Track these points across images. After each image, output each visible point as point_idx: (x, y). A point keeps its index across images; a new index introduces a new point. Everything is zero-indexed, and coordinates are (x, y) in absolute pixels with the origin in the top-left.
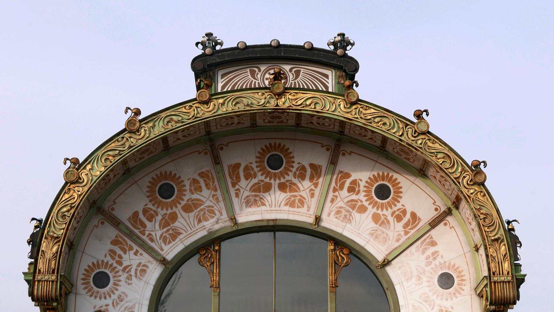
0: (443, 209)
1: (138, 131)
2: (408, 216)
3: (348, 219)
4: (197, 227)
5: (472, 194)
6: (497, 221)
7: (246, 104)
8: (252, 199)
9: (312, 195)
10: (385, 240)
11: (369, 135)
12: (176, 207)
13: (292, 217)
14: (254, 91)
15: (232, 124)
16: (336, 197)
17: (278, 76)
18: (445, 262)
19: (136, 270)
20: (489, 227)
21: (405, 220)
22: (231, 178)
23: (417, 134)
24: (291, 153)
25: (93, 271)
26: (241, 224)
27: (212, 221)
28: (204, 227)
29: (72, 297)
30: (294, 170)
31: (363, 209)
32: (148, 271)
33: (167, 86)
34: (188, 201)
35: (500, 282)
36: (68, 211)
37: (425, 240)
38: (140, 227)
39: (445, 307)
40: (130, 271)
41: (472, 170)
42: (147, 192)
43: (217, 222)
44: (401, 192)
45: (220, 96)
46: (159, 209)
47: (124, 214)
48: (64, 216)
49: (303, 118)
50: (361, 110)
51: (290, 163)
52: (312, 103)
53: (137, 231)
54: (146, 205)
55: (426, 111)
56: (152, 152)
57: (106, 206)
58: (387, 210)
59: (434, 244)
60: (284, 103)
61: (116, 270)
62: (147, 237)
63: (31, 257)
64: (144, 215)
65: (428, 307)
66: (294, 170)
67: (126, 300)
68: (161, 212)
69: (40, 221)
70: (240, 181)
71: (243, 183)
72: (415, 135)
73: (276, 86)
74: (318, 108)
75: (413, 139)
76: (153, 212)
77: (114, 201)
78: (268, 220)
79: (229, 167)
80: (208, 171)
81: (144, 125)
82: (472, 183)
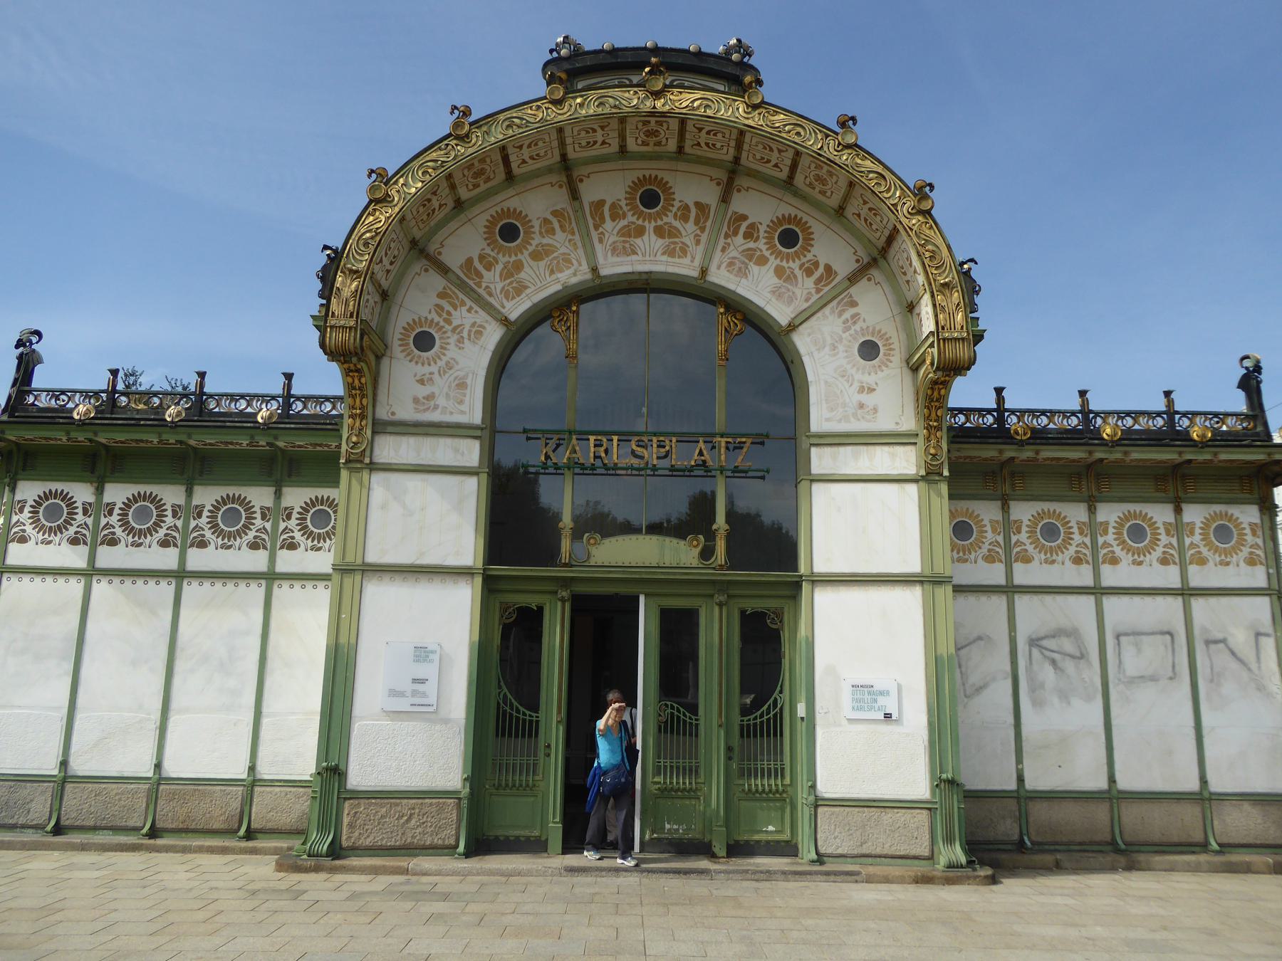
1: (467, 136)
2: (821, 269)
3: (743, 273)
4: (549, 279)
6: (948, 260)
8: (620, 246)
9: (698, 242)
10: (791, 300)
13: (671, 270)
19: (470, 331)
20: (937, 268)
21: (817, 274)
27: (568, 272)
29: (385, 362)
31: (762, 261)
32: (486, 333)
33: (511, 80)
36: (372, 238)
40: (462, 331)
41: (915, 195)
43: (575, 274)
46: (500, 256)
47: (453, 257)
48: (366, 244)
51: (670, 200)
53: (471, 283)
55: (853, 119)
57: (432, 248)
59: (854, 304)
63: (321, 296)
64: (481, 262)
66: (674, 210)
67: (457, 367)
68: (503, 259)
69: (335, 251)
71: (609, 225)
74: (709, 113)
78: (640, 273)
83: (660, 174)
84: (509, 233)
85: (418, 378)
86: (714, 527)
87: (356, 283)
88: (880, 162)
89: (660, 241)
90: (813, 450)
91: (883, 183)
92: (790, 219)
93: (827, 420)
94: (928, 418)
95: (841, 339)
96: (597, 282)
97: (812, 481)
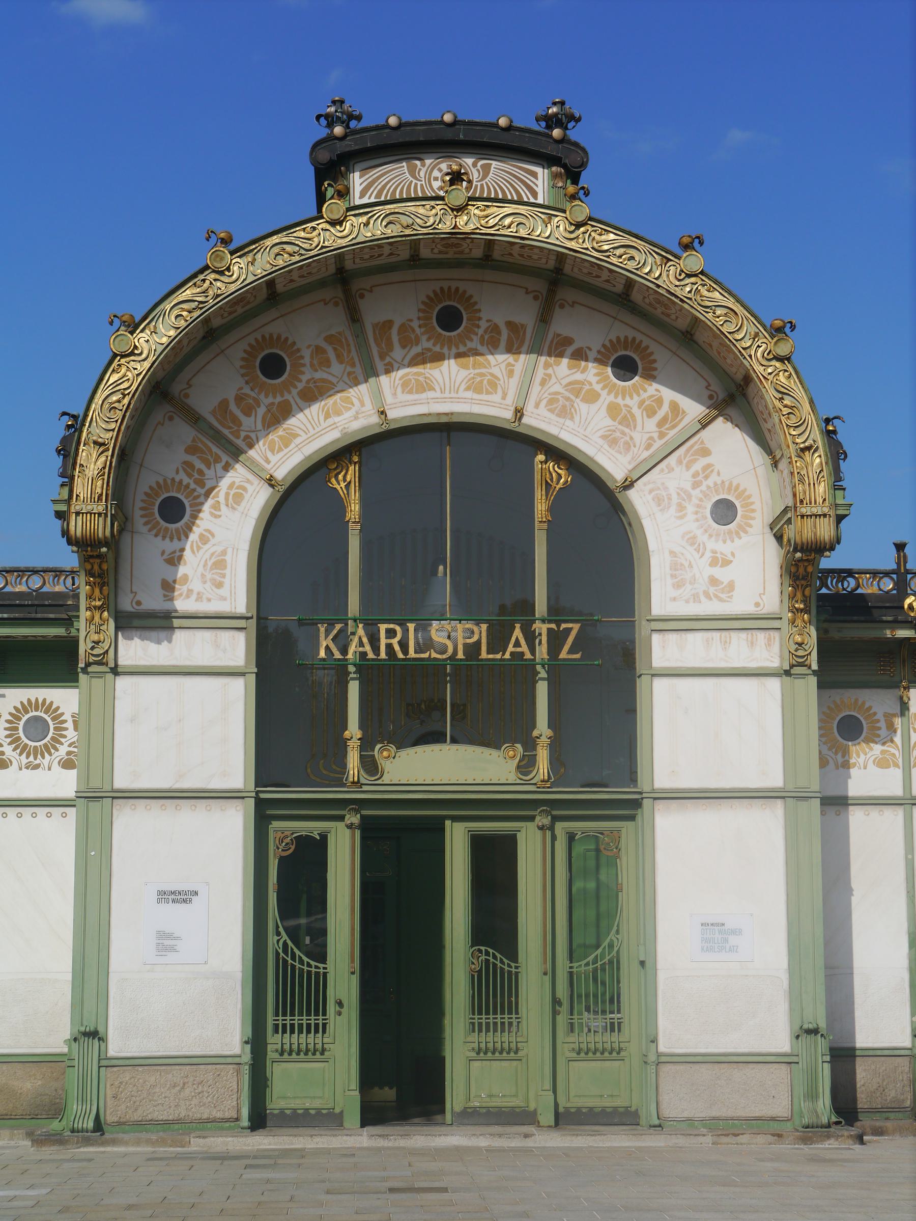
0: (722, 396)
1: (228, 269)
2: (666, 408)
4: (324, 425)
5: (770, 374)
7: (405, 225)
9: (511, 373)
11: (605, 275)
12: (290, 392)
13: (477, 409)
14: (418, 203)
15: (380, 256)
16: (550, 376)
17: (456, 177)
18: (723, 482)
19: (227, 494)
21: (661, 414)
22: (378, 345)
23: (683, 275)
24: (476, 303)
25: (157, 495)
26: (394, 420)
27: (348, 415)
28: (334, 426)
30: (480, 332)
31: (591, 397)
32: (247, 496)
34: (308, 382)
35: (811, 516)
36: (119, 401)
37: (692, 447)
38: (231, 425)
39: (722, 553)
41: (772, 337)
42: (241, 367)
44: (656, 369)
45: (361, 211)
46: (262, 396)
47: (204, 402)
49: (496, 247)
50: (593, 234)
52: (512, 223)
53: (226, 432)
54: (241, 388)
56: (248, 303)
58: (632, 398)
59: (705, 452)
60: (465, 223)
61: (196, 494)
62: (244, 440)
63: (62, 475)
65: (695, 553)
66: (480, 332)
67: (213, 541)
68: (266, 401)
69: (75, 417)
70: (392, 350)
72: (681, 277)
73: (454, 193)
74: (523, 233)
75: (678, 283)
76: (251, 401)
77: (188, 384)
78: (439, 414)
79: (375, 326)
80: (340, 333)
81: (238, 260)
82: (771, 356)
83: (462, 286)
84: (273, 367)
85: (165, 557)
86: (535, 733)
87: (102, 459)
88: (730, 293)
89: (464, 373)
90: (656, 637)
91: (734, 321)
92: (626, 343)
93: (674, 599)
94: (792, 597)
95: (690, 497)
96: (385, 428)
97: (653, 675)
